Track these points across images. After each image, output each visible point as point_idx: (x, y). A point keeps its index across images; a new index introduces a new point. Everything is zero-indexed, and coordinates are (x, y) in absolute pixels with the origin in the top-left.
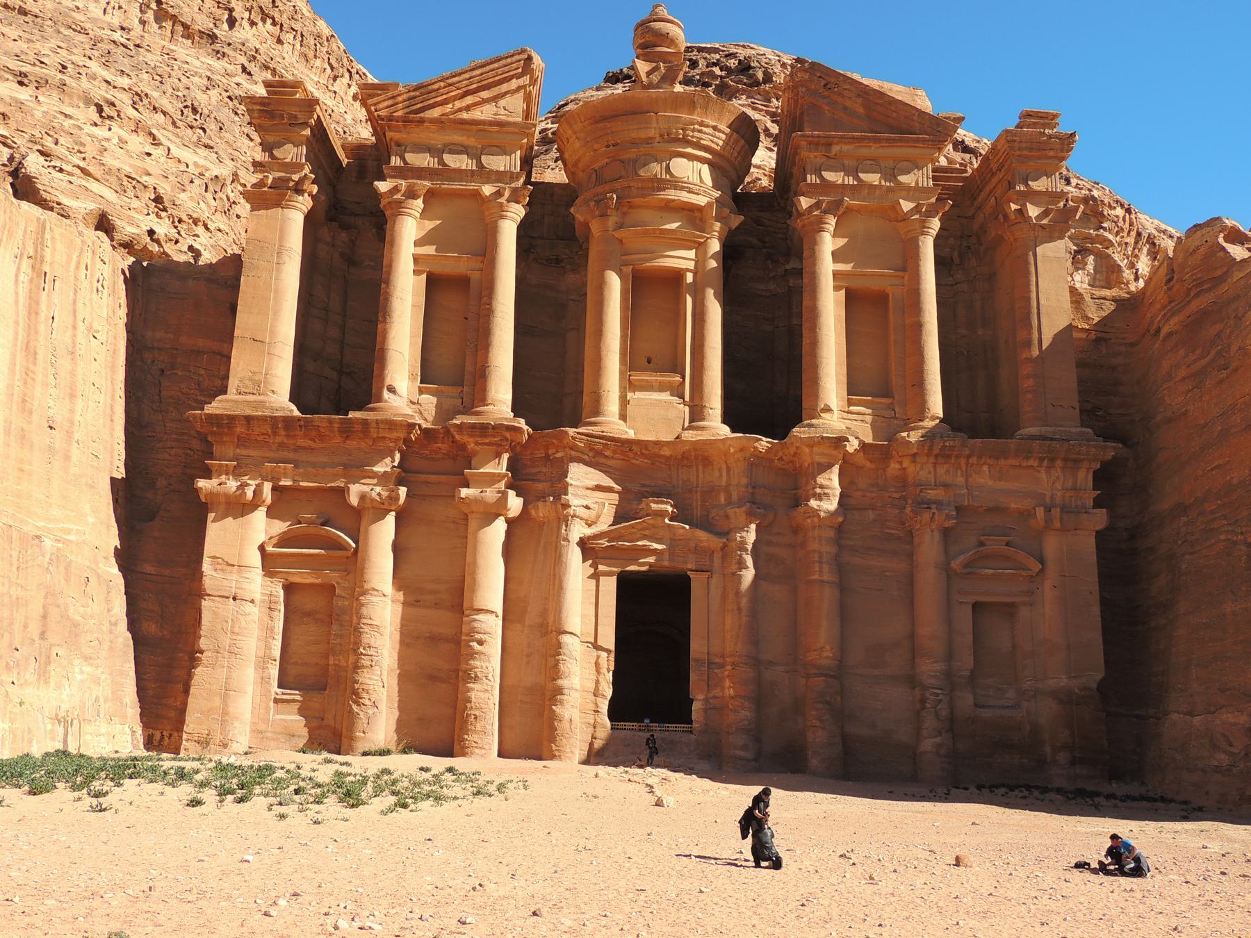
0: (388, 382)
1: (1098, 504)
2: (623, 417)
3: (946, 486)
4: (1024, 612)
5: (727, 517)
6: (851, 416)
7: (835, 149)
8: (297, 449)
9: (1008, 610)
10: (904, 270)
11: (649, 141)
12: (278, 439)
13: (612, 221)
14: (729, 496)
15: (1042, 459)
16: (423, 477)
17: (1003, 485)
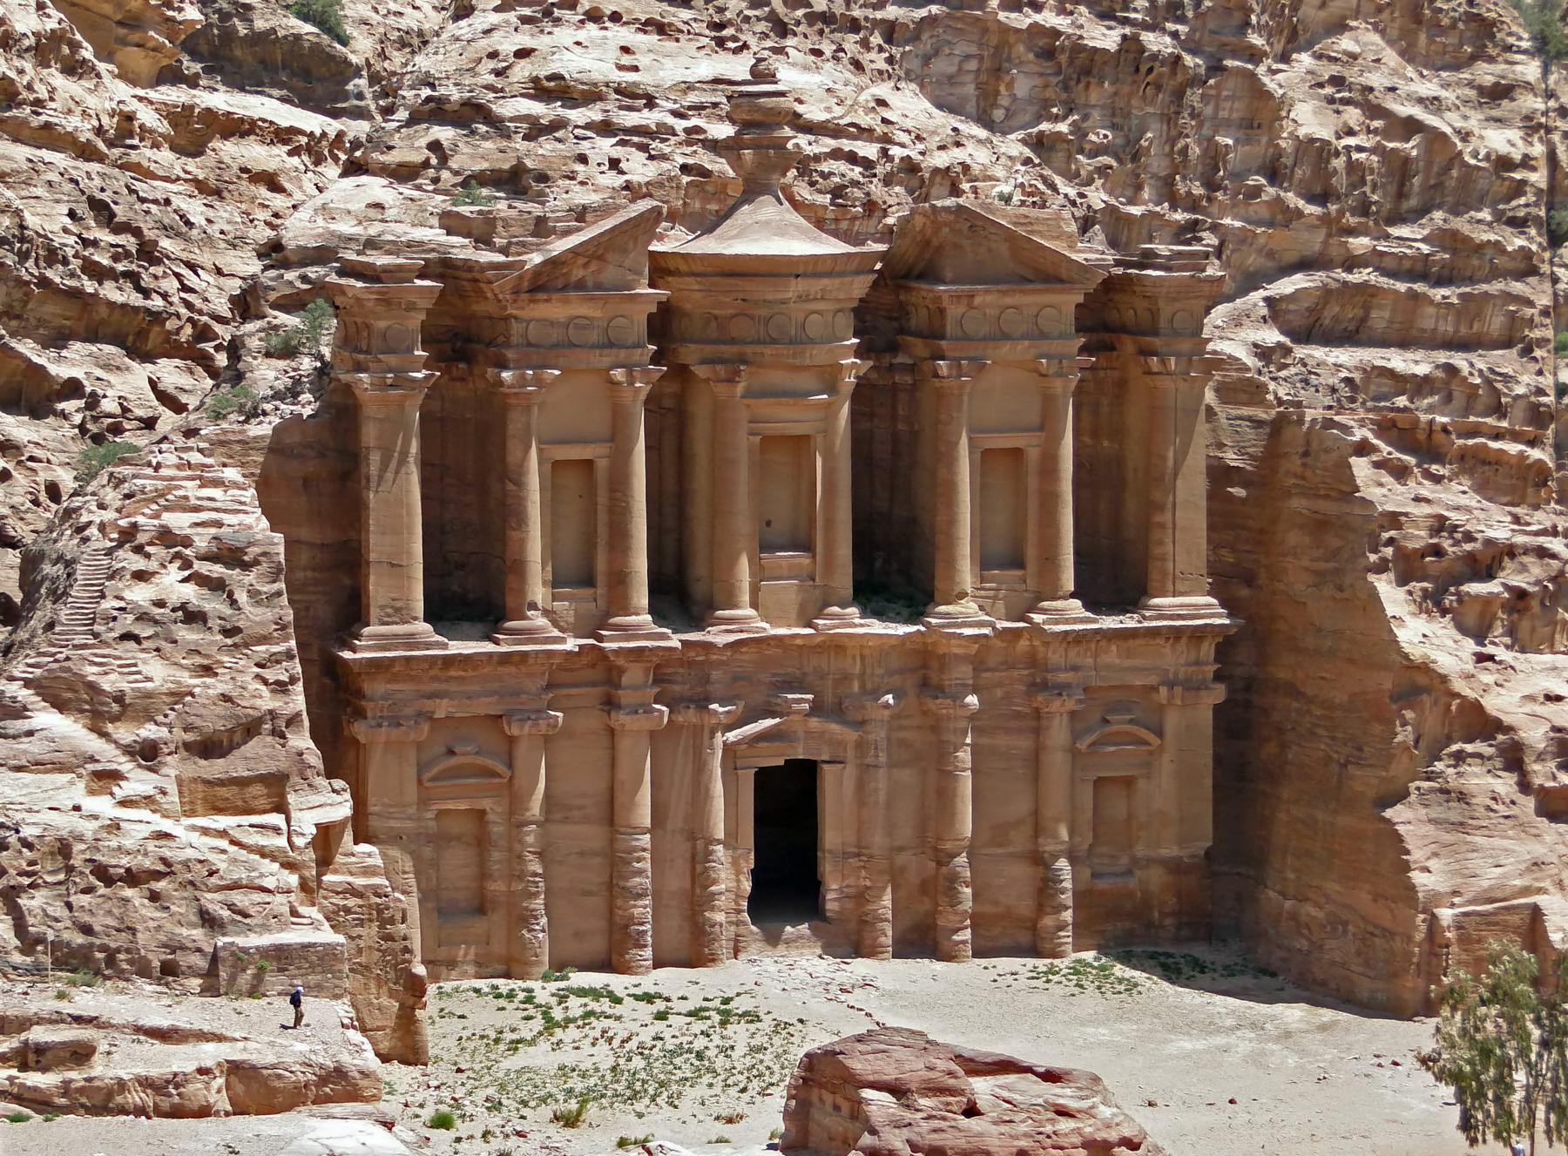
0: (530, 598)
1: (1218, 677)
2: (754, 605)
3: (1075, 668)
4: (1142, 784)
5: (863, 707)
6: (983, 593)
7: (978, 300)
8: (448, 680)
9: (1128, 782)
10: (1041, 428)
11: (784, 302)
12: (432, 673)
13: (740, 388)
14: (863, 686)
15: (1168, 639)
16: (564, 691)
17: (1128, 663)
